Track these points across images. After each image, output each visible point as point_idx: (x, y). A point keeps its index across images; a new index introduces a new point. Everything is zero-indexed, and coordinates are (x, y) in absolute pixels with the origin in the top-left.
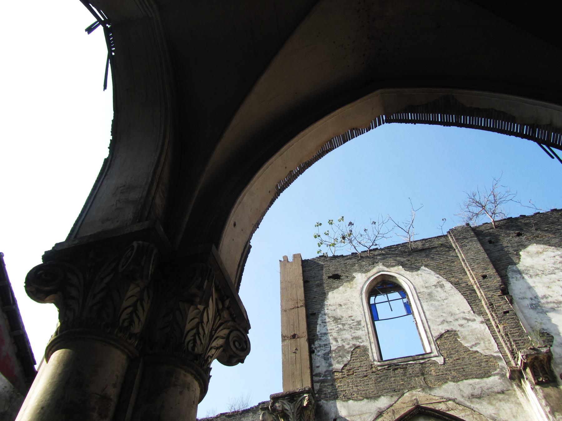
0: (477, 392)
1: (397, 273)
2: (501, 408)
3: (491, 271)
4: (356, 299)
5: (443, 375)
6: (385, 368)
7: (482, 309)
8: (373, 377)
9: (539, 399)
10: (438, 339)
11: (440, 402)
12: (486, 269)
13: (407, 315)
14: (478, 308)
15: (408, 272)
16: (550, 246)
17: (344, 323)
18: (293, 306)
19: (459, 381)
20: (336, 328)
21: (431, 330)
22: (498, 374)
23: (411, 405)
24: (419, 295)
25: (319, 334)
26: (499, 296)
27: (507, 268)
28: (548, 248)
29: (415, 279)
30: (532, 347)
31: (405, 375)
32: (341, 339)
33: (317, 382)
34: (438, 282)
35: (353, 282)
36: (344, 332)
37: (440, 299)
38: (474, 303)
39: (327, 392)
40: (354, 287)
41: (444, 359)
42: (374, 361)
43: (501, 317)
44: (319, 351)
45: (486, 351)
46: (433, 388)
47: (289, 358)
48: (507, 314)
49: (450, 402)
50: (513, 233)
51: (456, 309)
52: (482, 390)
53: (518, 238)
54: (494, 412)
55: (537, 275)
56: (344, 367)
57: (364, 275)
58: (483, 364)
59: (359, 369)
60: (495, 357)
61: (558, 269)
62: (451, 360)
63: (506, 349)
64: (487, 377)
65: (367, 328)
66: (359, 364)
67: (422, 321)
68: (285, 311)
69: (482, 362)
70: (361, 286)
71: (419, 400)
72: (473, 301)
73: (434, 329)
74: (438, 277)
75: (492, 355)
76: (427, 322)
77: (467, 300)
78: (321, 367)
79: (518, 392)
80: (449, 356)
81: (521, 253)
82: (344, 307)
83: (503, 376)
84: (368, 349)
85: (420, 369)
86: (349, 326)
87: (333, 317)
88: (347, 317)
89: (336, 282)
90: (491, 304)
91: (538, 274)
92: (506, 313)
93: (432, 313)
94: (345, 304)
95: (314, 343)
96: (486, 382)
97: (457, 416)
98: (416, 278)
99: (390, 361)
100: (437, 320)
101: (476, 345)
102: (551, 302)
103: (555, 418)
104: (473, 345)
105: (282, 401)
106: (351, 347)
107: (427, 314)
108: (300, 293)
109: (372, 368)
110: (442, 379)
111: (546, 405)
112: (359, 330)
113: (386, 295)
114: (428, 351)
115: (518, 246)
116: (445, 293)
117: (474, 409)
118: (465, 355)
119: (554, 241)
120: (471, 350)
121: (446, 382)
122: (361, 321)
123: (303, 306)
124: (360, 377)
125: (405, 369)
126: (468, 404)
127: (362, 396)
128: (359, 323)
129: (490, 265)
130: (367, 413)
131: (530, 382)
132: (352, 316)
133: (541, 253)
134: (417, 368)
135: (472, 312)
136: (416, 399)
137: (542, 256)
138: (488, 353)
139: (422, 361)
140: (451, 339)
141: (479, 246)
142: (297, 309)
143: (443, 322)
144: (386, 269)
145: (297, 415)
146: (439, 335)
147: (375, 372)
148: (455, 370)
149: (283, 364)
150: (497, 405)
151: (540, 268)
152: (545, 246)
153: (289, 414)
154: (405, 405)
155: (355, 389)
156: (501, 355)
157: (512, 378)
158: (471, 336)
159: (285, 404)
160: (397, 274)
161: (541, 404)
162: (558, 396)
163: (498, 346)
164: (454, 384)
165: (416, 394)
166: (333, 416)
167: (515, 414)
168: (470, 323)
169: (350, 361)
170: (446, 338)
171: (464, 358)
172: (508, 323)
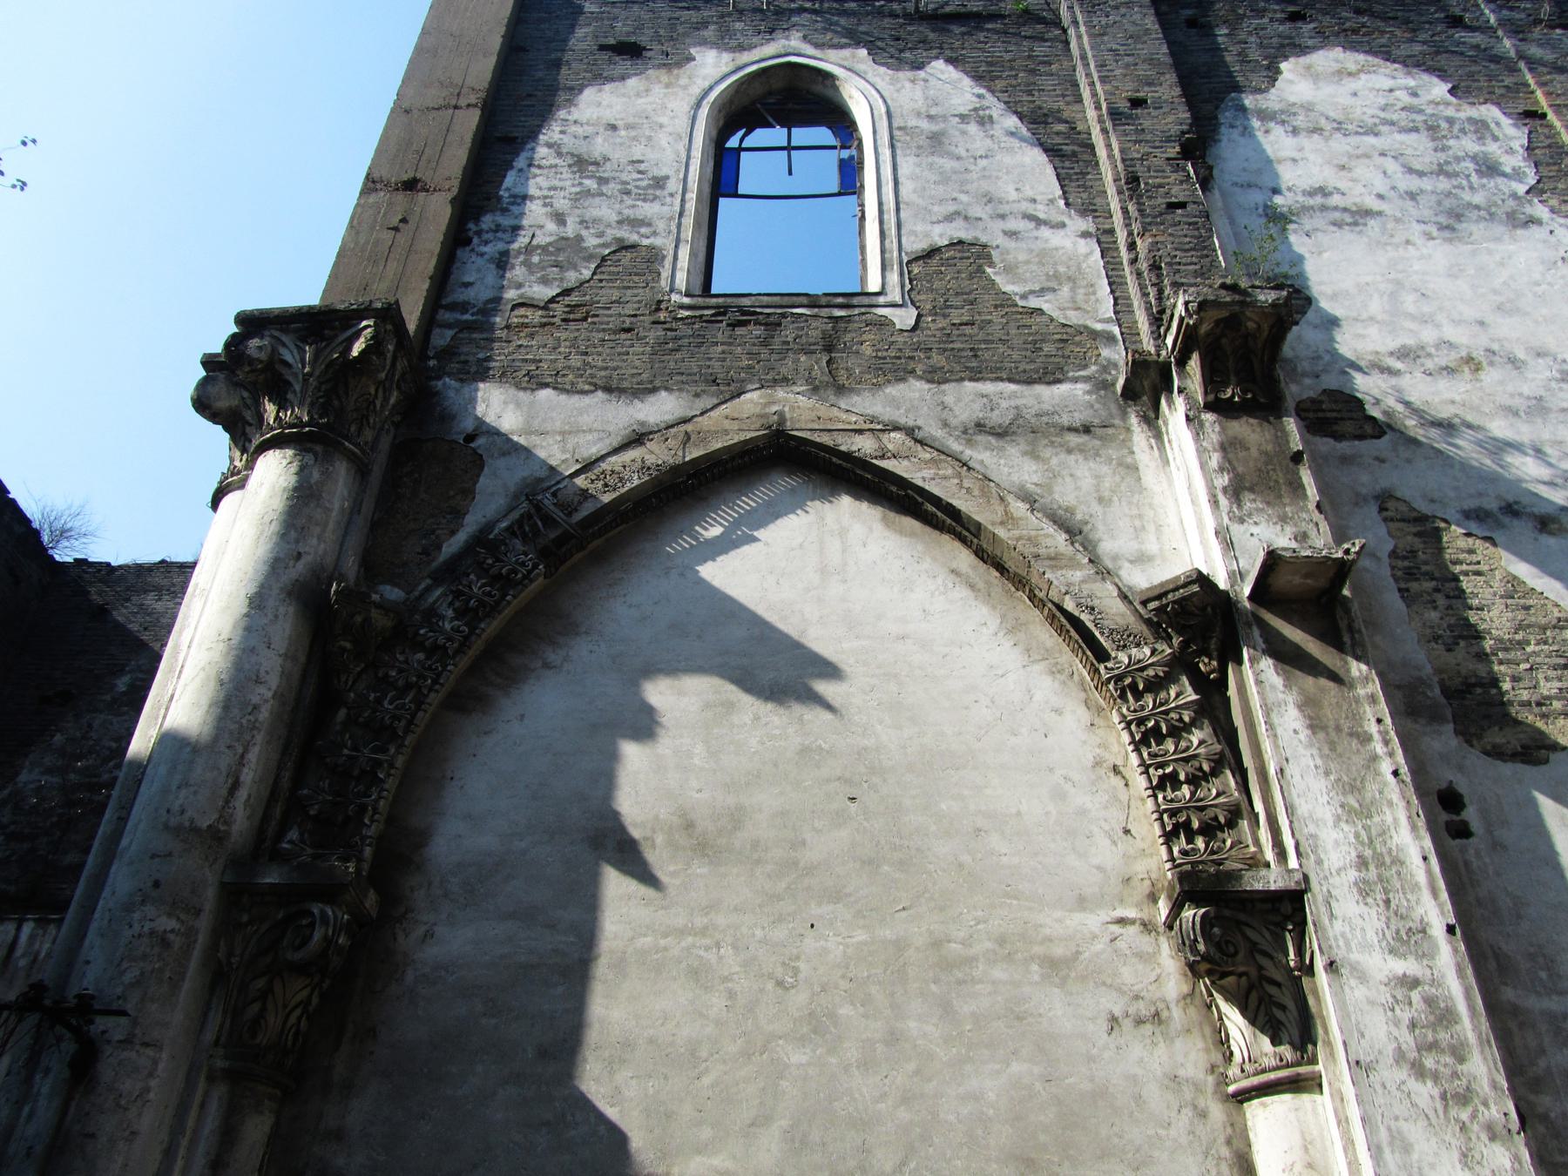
0: (996, 418)
1: (845, 68)
2: (1064, 473)
3: (1168, 89)
4: (673, 118)
5: (899, 358)
6: (701, 316)
7: (1098, 201)
8: (656, 334)
9: (1201, 451)
10: (917, 259)
11: (860, 432)
12: (1150, 84)
13: (839, 194)
14: (1085, 196)
15: (883, 70)
16: (1388, 60)
17: (606, 175)
18: (441, 102)
19: (946, 381)
20: (573, 185)
21: (903, 232)
22: (1087, 379)
23: (758, 426)
24: (896, 133)
25: (506, 195)
26: (1168, 159)
27: (1222, 100)
28: (1380, 66)
29: (898, 91)
30: (1229, 281)
31: (765, 343)
32: (578, 220)
33: (449, 326)
34: (975, 109)
35: (681, 71)
36: (597, 200)
37: (963, 153)
38: (1078, 180)
39: (471, 358)
40: (680, 86)
41: (919, 316)
42: (672, 290)
43: (1156, 217)
44: (486, 243)
45: (1071, 313)
46: (851, 390)
47: (367, 242)
48: (1179, 211)
49: (896, 436)
50: (1275, 11)
51: (1011, 189)
52: (1019, 416)
53: (1288, 25)
54: (1035, 479)
55: (1317, 130)
56: (558, 295)
57: (726, 57)
58: (1048, 348)
59: (609, 308)
60: (1094, 335)
61: (1392, 123)
62: (942, 323)
63: (1137, 302)
64: (1049, 383)
65: (683, 201)
66: (615, 295)
67: (880, 204)
68: (407, 112)
69: (1043, 341)
70: (707, 84)
71: (788, 416)
72: (1076, 174)
73: (914, 233)
74: (979, 96)
75: (1086, 327)
76: (898, 210)
77: (1055, 168)
78: (476, 287)
79: (1140, 436)
80: (941, 310)
81: (1284, 66)
82: (623, 133)
83: (1105, 386)
84: (664, 257)
85: (823, 332)
86: (619, 187)
87: (572, 155)
88: (624, 161)
89: (623, 64)
90: (1133, 180)
91: (1322, 129)
92: (1172, 206)
93: (924, 188)
94: (628, 127)
95: (477, 220)
96: (1038, 398)
97: (905, 475)
98: (903, 87)
99: (729, 300)
100: (936, 208)
101: (1042, 292)
102: (1336, 208)
103: (1239, 506)
104: (1032, 292)
105: (277, 334)
106: (604, 245)
107: (905, 191)
108: (482, 70)
109: (658, 310)
110: (892, 368)
111: (1221, 469)
112: (652, 201)
113: (786, 130)
114: (874, 285)
115: (1282, 46)
116: (989, 141)
117: (971, 464)
118: (996, 318)
119: (1404, 50)
120: (1021, 303)
121: (902, 380)
122: (667, 177)
123: (475, 106)
124: (604, 330)
125: (773, 325)
126: (955, 446)
127: (590, 384)
128: (660, 182)
129: (1168, 76)
130: (590, 431)
131: (1189, 400)
132: (642, 162)
133: (1350, 74)
134: (815, 331)
135: (1062, 203)
136: (781, 414)
137: (1351, 85)
138: (1074, 318)
139: (838, 313)
140: (961, 265)
141: (1151, 22)
142: (451, 111)
143: (949, 218)
144: (810, 50)
145: (321, 383)
146: (923, 250)
147: (664, 323)
148: (945, 350)
149: (340, 255)
150: (1054, 461)
151: (1332, 114)
152: (1370, 58)
153: (290, 379)
154: (735, 426)
155: (576, 361)
156: (1116, 330)
157: (1130, 393)
158: (1035, 268)
159: (284, 345)
160: (842, 70)
161: (1203, 466)
162: (1270, 448)
163: (1116, 304)
164: (927, 386)
165: (786, 400)
166: (469, 425)
167: (1106, 494)
168: (1045, 232)
169: (588, 281)
170: (947, 263)
171: (990, 322)
172: (1170, 235)
